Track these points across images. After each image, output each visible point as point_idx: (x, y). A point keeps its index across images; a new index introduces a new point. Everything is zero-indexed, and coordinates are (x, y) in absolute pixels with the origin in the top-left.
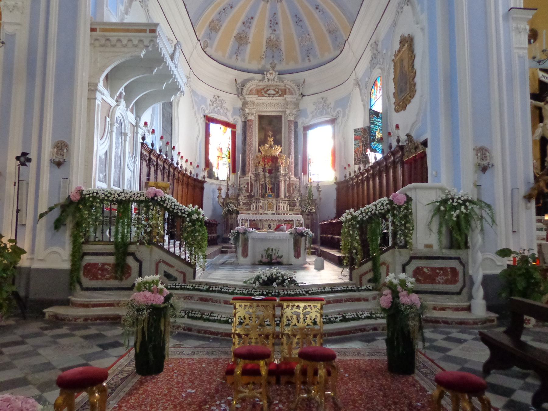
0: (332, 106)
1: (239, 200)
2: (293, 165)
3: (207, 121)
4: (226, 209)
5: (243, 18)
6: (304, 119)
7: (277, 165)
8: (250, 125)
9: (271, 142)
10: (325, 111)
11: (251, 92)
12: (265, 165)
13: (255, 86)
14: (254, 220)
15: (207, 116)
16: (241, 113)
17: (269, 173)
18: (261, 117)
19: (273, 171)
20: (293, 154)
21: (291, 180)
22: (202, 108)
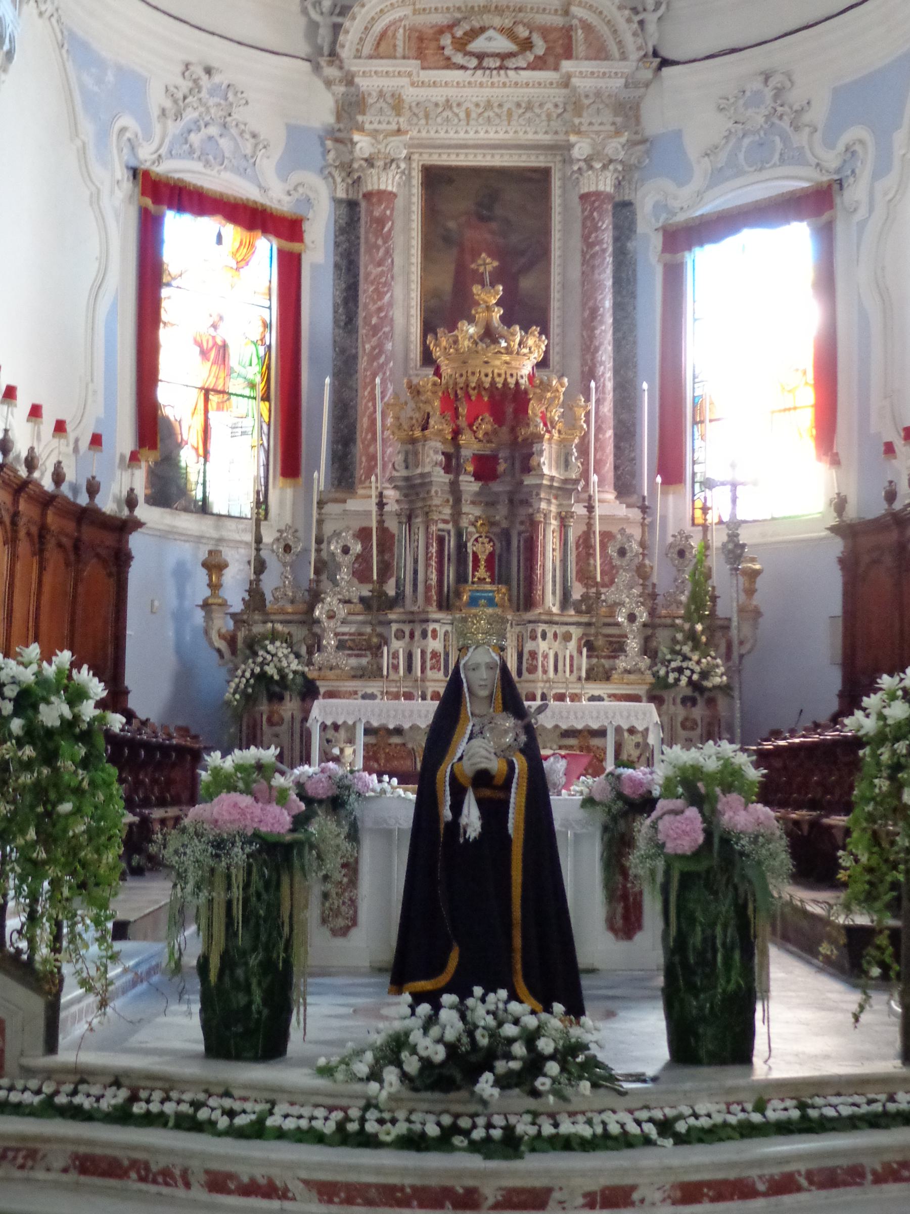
0: (818, 114)
1: (318, 621)
2: (610, 433)
3: (148, 202)
4: (249, 668)
6: (668, 185)
7: (523, 432)
8: (381, 222)
9: (488, 309)
10: (779, 144)
12: (457, 433)
14: (398, 731)
15: (146, 174)
16: (331, 156)
17: (477, 476)
19: (502, 467)
20: (609, 374)
21: (597, 512)
22: (123, 130)
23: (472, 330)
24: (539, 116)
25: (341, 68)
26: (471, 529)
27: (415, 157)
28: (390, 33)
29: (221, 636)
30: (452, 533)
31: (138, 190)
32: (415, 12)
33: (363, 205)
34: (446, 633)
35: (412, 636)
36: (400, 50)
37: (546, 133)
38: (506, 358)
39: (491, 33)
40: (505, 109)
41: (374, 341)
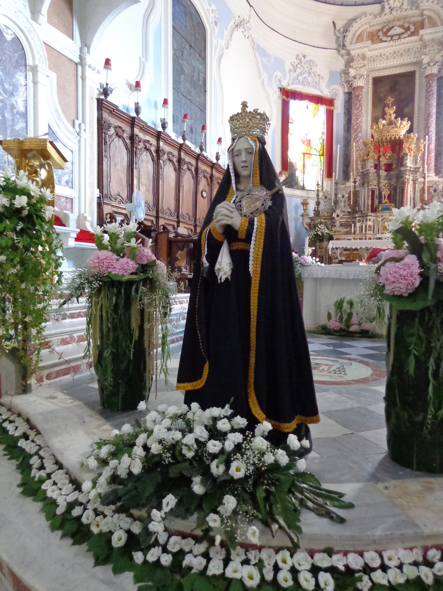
1: (334, 218)
2: (433, 154)
3: (285, 97)
4: (313, 233)
7: (402, 154)
8: (358, 96)
9: (390, 115)
11: (359, 39)
12: (379, 157)
13: (367, 26)
14: (356, 249)
15: (284, 89)
17: (386, 170)
18: (377, 81)
19: (394, 166)
20: (434, 135)
21: (427, 179)
23: (384, 122)
24: (411, 53)
25: (346, 50)
26: (384, 188)
27: (370, 75)
28: (362, 35)
29: (307, 224)
30: (377, 189)
31: (282, 94)
32: (370, 26)
33: (353, 92)
34: (374, 220)
35: (363, 221)
36: (365, 39)
37: (414, 58)
38: (396, 129)
39: (395, 28)
40: (400, 53)
41: (355, 134)
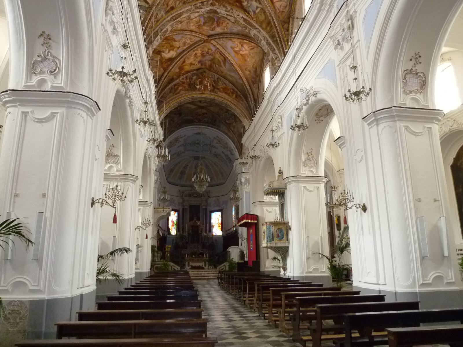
5: (184, 165)
11: (186, 196)
